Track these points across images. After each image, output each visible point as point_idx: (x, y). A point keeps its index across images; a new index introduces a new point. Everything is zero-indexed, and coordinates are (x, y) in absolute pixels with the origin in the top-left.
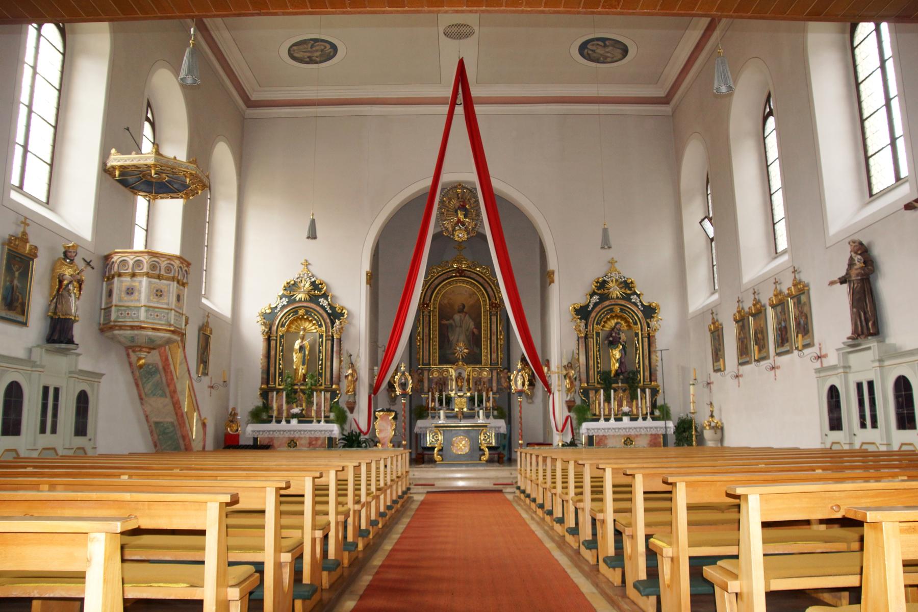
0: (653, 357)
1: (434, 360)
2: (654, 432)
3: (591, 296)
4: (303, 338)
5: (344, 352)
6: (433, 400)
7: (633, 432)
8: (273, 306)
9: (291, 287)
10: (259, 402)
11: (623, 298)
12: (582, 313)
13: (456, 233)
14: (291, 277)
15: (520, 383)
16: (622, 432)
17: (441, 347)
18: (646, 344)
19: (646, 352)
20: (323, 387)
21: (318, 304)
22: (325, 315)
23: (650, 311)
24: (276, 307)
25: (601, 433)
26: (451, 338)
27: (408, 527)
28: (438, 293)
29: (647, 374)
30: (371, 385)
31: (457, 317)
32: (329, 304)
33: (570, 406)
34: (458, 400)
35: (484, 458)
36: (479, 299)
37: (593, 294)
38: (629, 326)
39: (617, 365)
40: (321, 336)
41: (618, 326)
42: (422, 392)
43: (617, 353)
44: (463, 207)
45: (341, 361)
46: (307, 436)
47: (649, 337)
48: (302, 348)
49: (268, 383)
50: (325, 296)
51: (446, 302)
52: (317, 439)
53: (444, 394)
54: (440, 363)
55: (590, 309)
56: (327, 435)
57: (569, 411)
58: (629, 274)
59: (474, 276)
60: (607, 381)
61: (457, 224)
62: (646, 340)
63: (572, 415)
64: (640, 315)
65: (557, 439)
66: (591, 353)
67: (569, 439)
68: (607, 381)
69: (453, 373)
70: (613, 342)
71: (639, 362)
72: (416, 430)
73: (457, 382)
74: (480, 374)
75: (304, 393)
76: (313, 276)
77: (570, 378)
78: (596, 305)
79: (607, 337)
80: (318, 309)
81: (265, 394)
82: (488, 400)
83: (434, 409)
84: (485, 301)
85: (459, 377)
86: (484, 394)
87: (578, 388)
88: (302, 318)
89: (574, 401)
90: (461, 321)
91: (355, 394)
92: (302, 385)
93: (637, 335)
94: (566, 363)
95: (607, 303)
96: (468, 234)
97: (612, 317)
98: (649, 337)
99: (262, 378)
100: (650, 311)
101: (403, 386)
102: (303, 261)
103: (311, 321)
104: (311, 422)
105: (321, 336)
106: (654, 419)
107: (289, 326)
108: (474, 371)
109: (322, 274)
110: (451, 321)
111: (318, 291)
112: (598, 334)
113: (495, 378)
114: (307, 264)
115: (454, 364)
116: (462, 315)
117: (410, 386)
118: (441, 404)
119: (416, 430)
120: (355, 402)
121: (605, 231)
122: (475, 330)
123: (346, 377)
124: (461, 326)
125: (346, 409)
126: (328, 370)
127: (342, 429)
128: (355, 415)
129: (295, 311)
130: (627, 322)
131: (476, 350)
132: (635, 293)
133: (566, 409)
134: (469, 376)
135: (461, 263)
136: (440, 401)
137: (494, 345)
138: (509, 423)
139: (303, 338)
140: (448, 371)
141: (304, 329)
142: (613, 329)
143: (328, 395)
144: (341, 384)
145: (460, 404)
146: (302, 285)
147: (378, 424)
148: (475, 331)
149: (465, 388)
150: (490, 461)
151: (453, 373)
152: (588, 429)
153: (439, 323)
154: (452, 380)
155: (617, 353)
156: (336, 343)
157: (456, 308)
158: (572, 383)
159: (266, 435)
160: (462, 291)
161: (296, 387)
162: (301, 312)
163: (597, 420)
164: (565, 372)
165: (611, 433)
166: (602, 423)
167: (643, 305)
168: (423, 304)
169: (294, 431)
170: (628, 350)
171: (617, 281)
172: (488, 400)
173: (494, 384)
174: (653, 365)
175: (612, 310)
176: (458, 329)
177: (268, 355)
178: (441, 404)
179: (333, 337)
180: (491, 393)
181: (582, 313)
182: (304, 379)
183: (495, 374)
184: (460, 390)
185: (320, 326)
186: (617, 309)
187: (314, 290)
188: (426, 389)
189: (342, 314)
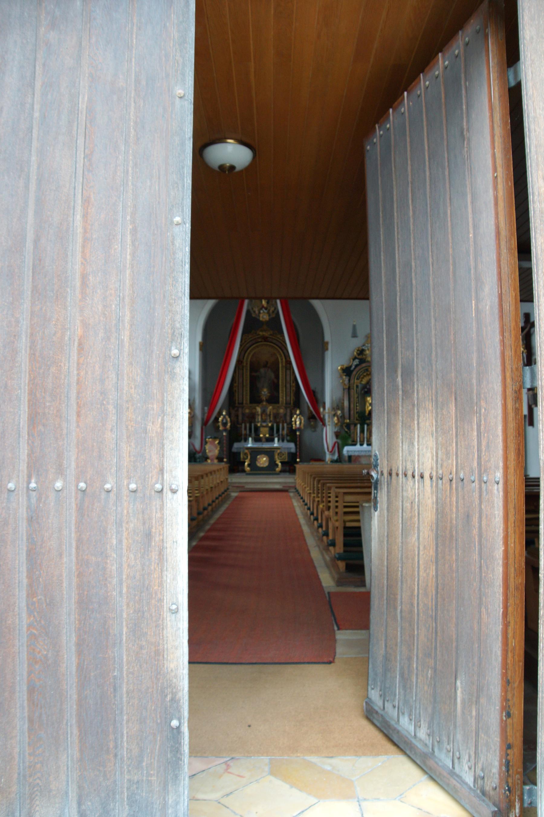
3: (354, 360)
13: (261, 315)
15: (298, 423)
25: (356, 454)
27: (228, 509)
30: (203, 419)
31: (262, 370)
33: (337, 435)
34: (262, 429)
35: (278, 469)
36: (278, 358)
53: (253, 425)
55: (352, 369)
61: (261, 309)
63: (339, 441)
65: (328, 457)
66: (352, 399)
67: (336, 457)
69: (259, 410)
72: (234, 450)
78: (356, 366)
82: (283, 429)
84: (282, 359)
85: (264, 412)
86: (281, 425)
95: (364, 365)
96: (269, 315)
101: (225, 424)
119: (234, 450)
121: (354, 327)
134: (270, 412)
147: (207, 447)
148: (275, 381)
150: (283, 471)
151: (259, 410)
153: (250, 375)
154: (258, 415)
160: (265, 353)
163: (355, 445)
164: (333, 413)
165: (363, 454)
168: (239, 362)
172: (283, 429)
180: (285, 425)
181: (347, 371)
183: (288, 411)
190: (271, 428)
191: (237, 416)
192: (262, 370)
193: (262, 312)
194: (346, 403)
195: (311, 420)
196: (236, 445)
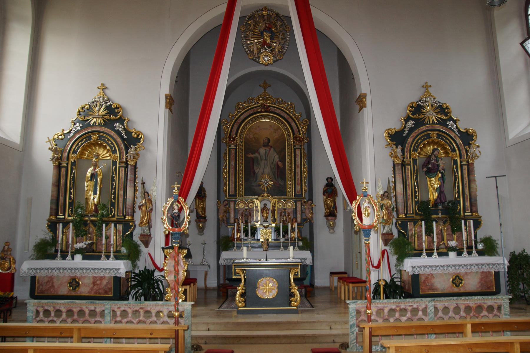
0: (473, 185)
1: (239, 192)
2: (485, 270)
4: (95, 165)
5: (139, 181)
6: (239, 231)
7: (462, 270)
8: (65, 132)
9: (85, 112)
10: (45, 234)
11: (439, 123)
12: (397, 138)
13: (262, 56)
14: (86, 100)
16: (452, 270)
17: (246, 180)
18: (466, 172)
19: (466, 180)
20: (115, 219)
21: (113, 129)
22: (119, 140)
23: (468, 138)
24: (70, 132)
25: (428, 271)
26: (257, 171)
28: (244, 128)
29: (468, 204)
31: (262, 151)
32: (125, 129)
33: (387, 238)
37: (407, 119)
38: (446, 153)
39: (436, 194)
40: (114, 163)
41: (436, 153)
42: (228, 222)
43: (435, 183)
44: (268, 29)
45: (135, 190)
46: (90, 275)
47: (468, 164)
48: (93, 176)
49: (57, 214)
50: (121, 120)
51: (251, 136)
52: (102, 278)
53: (249, 224)
54: (246, 195)
56: (113, 274)
57: (386, 245)
58: (443, 99)
59: (279, 112)
60: (426, 212)
62: (465, 167)
64: (459, 141)
66: (409, 182)
68: (426, 212)
69: (258, 204)
70: (430, 168)
71: (458, 192)
73: (262, 212)
74: (285, 205)
75: (95, 225)
76: (109, 100)
77: (387, 209)
78: (411, 130)
79: (425, 164)
80: (112, 133)
81: (52, 226)
83: (239, 239)
84: (289, 135)
85: (264, 209)
87: (394, 221)
88: (96, 144)
89: (392, 234)
90: (267, 154)
91: (150, 227)
92: (93, 216)
93: (455, 162)
94: (381, 193)
95: (423, 128)
97: (429, 144)
98: (468, 164)
99: (51, 208)
100: (468, 138)
102: (100, 85)
103: (105, 147)
104: (99, 258)
105: (114, 163)
106: (481, 253)
107: (82, 153)
108: (279, 202)
109: (117, 97)
110: (257, 155)
111: (114, 114)
112: (415, 161)
113: (299, 209)
114: (104, 88)
115: (259, 195)
116: (268, 149)
117: (186, 220)
118: (247, 235)
119: (221, 262)
120: (150, 235)
122: (280, 163)
123: (140, 207)
124: (266, 160)
125: (139, 242)
126: (121, 200)
127: (134, 266)
128: (150, 249)
129: (88, 136)
130: (444, 148)
131: (281, 183)
132: (451, 119)
134: (274, 207)
135: (266, 100)
136: (246, 231)
137: (298, 177)
138: (312, 252)
139: (95, 165)
140: (253, 202)
141: (98, 156)
142: (429, 157)
143: (120, 227)
144: (136, 215)
145: (265, 234)
146: (97, 108)
148: (280, 164)
149: (270, 219)
152: (413, 267)
155: (435, 183)
156: (130, 169)
157: (262, 142)
158: (389, 214)
159: (44, 274)
161: (87, 218)
162: (94, 137)
163: (419, 255)
165: (439, 271)
166: (423, 261)
167: (459, 131)
169: (76, 269)
170: (447, 178)
171: (432, 106)
173: (299, 216)
174: (473, 194)
175: (429, 136)
176: (263, 162)
177: (57, 184)
178: (247, 235)
179: (127, 163)
180: (296, 225)
181: (397, 138)
182: (96, 210)
184: (266, 221)
185: (114, 152)
186: (434, 135)
187: (109, 114)
188: (232, 220)
189: (138, 140)
190: (277, 230)
191: (227, 212)
192: (262, 151)
193: (263, 50)
194: (400, 188)
195: (330, 218)
196: (225, 255)
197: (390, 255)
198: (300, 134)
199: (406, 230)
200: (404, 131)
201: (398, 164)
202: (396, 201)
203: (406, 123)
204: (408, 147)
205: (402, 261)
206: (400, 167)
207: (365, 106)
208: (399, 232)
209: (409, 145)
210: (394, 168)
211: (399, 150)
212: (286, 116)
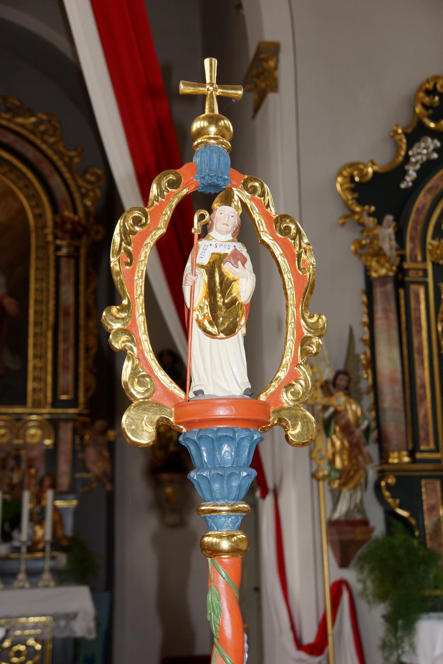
3: (417, 132)
33: (346, 538)
36: (22, 210)
37: (417, 132)
57: (344, 563)
77: (347, 430)
78: (427, 169)
87: (372, 475)
89: (365, 523)
133: (329, 558)
148: (10, 304)
158: (354, 450)
172: (38, 518)
173: (64, 467)
194: (389, 360)
195: (165, 476)
197: (362, 606)
198: (75, 212)
199: (415, 506)
200: (405, 173)
201: (383, 279)
202: (376, 406)
203: (410, 146)
204: (416, 222)
205: (409, 628)
206: (390, 287)
207: (274, 87)
208: (390, 514)
209: (422, 217)
210: (369, 291)
211: (386, 233)
212: (31, 153)
